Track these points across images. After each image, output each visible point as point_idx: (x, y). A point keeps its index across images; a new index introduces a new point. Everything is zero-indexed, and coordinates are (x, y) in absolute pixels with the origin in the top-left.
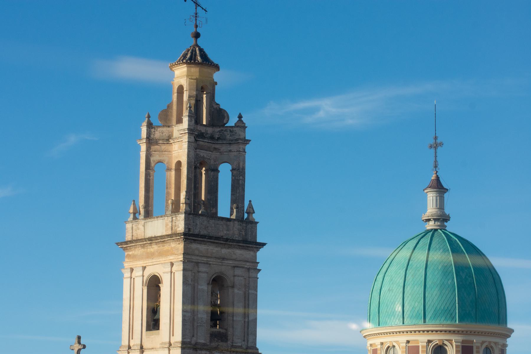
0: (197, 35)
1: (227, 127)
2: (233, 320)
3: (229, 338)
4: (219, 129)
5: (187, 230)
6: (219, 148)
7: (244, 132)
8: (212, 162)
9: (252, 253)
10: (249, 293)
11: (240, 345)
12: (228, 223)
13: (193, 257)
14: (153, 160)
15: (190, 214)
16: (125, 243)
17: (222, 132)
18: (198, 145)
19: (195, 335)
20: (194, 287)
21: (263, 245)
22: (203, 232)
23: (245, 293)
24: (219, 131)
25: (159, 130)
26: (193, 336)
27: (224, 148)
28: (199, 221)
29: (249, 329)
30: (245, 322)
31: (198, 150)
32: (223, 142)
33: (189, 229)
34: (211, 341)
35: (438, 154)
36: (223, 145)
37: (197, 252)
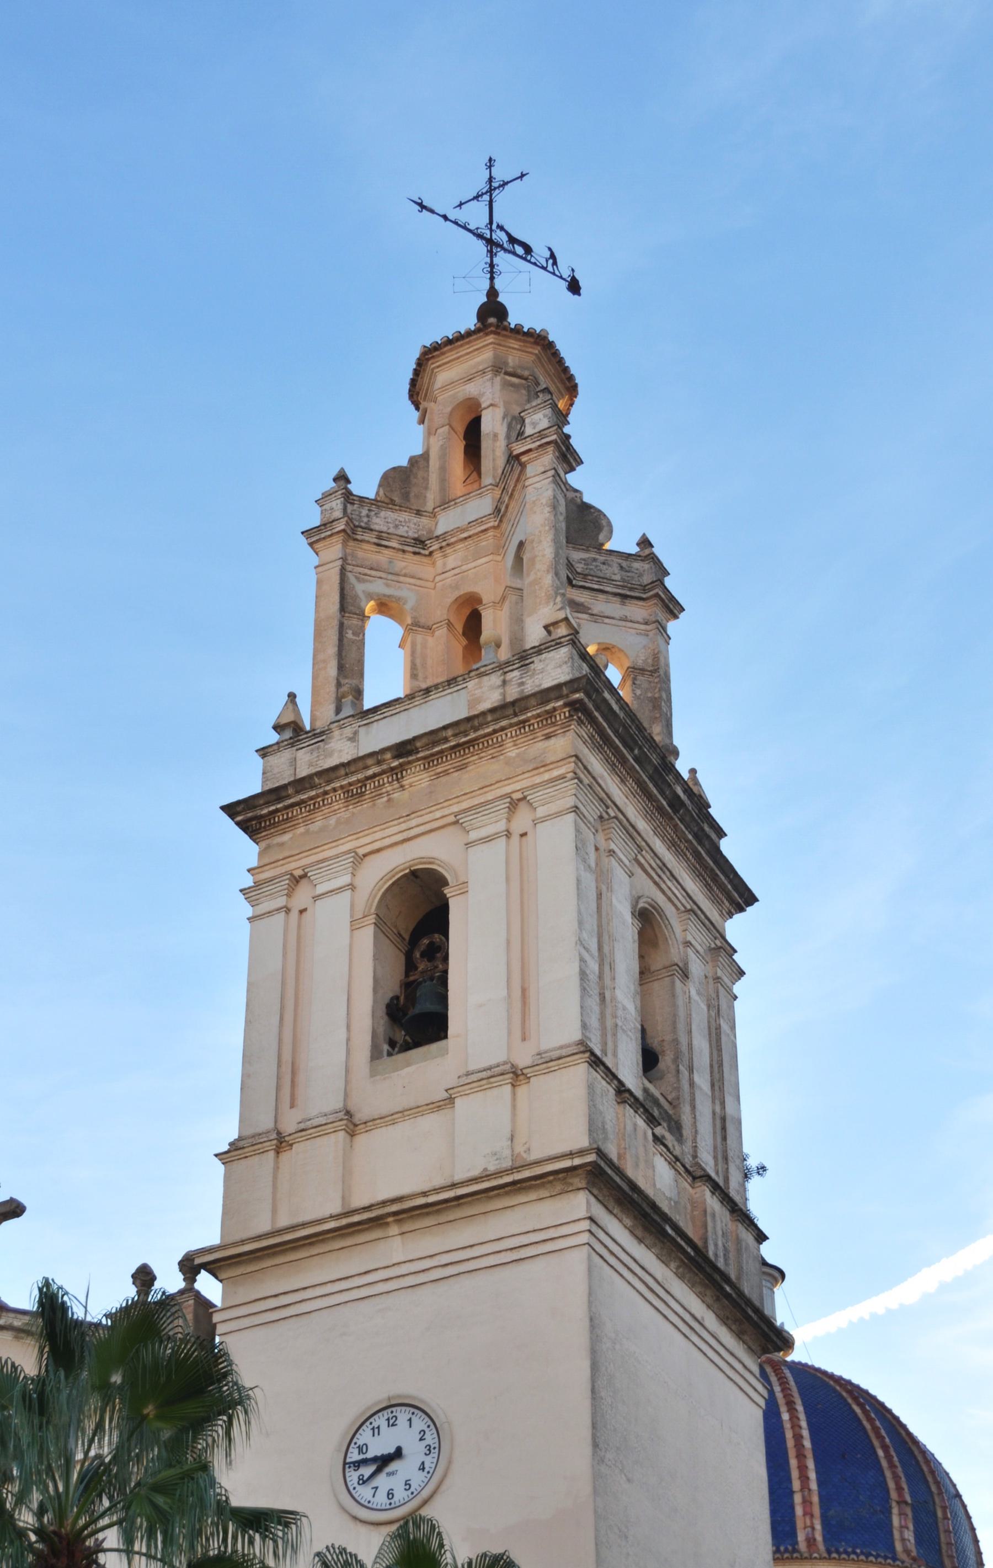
1: (611, 552)
6: (586, 604)
14: (363, 591)
16: (273, 797)
17: (594, 563)
19: (609, 1054)
24: (584, 560)
25: (383, 514)
32: (601, 587)
36: (601, 596)
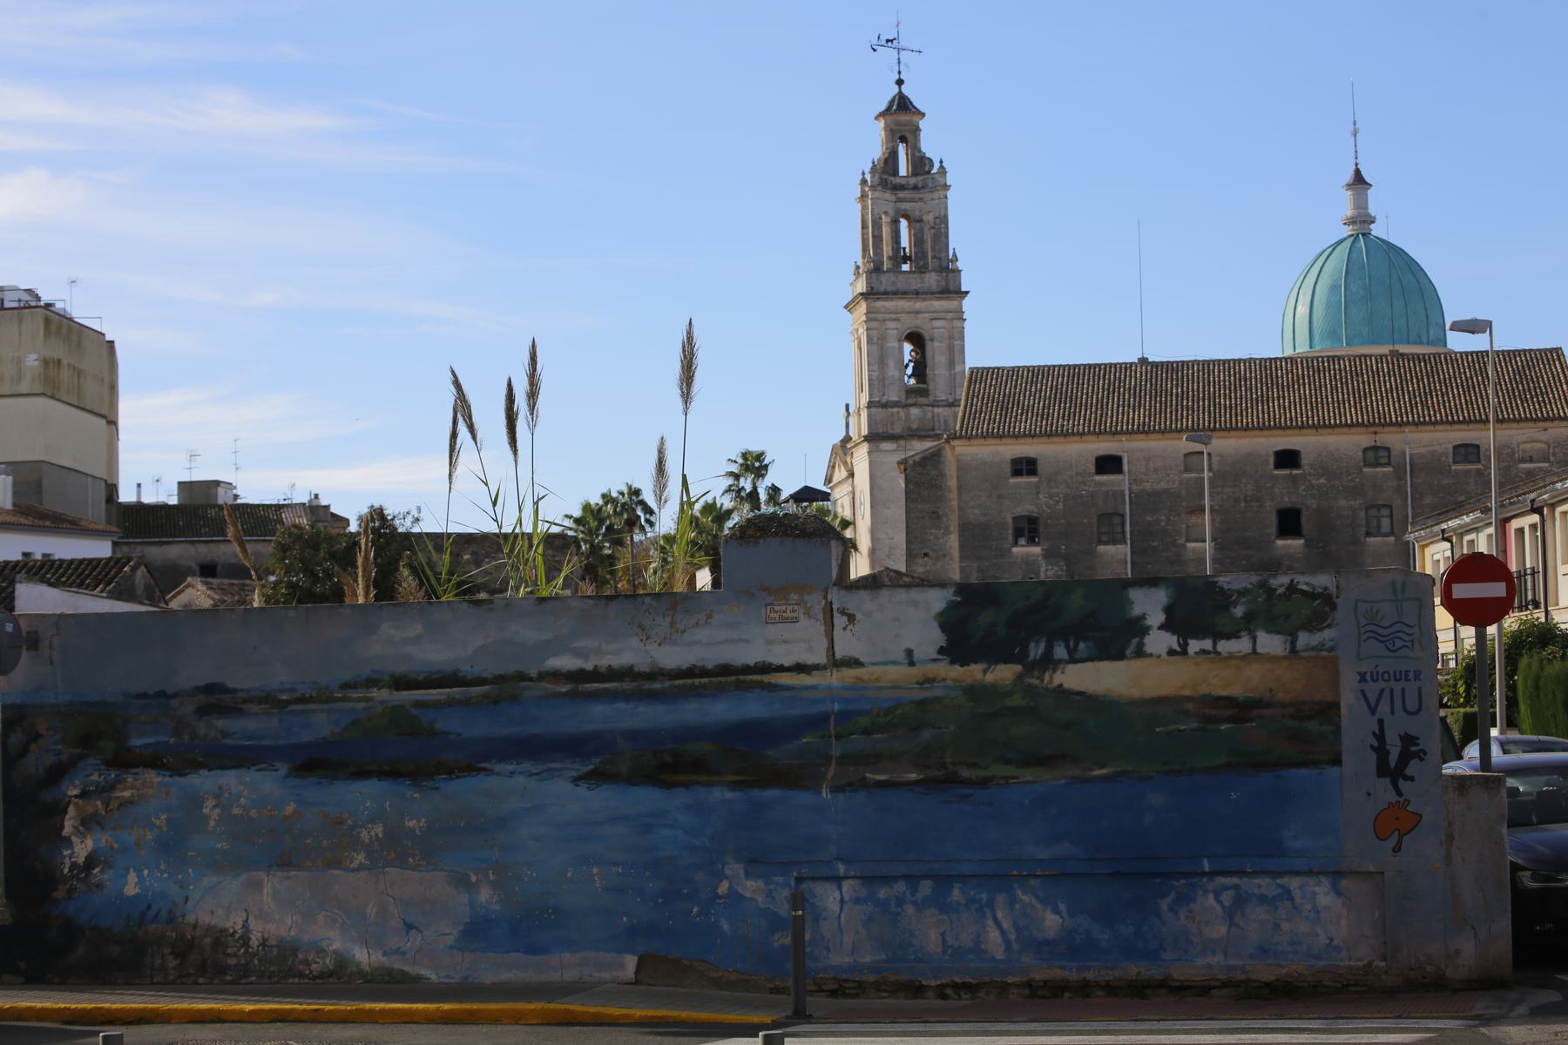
0: (900, 82)
2: (934, 374)
3: (930, 392)
4: (920, 178)
5: (869, 289)
7: (945, 177)
8: (917, 213)
9: (956, 303)
10: (953, 346)
11: (944, 398)
12: (923, 275)
13: (877, 315)
15: (871, 272)
18: (898, 198)
20: (882, 346)
21: (967, 293)
22: (890, 289)
23: (949, 345)
26: (884, 395)
27: (927, 197)
28: (884, 278)
29: (957, 381)
30: (951, 375)
31: (898, 204)
33: (872, 288)
34: (907, 398)
35: (1358, 143)
37: (883, 310)
